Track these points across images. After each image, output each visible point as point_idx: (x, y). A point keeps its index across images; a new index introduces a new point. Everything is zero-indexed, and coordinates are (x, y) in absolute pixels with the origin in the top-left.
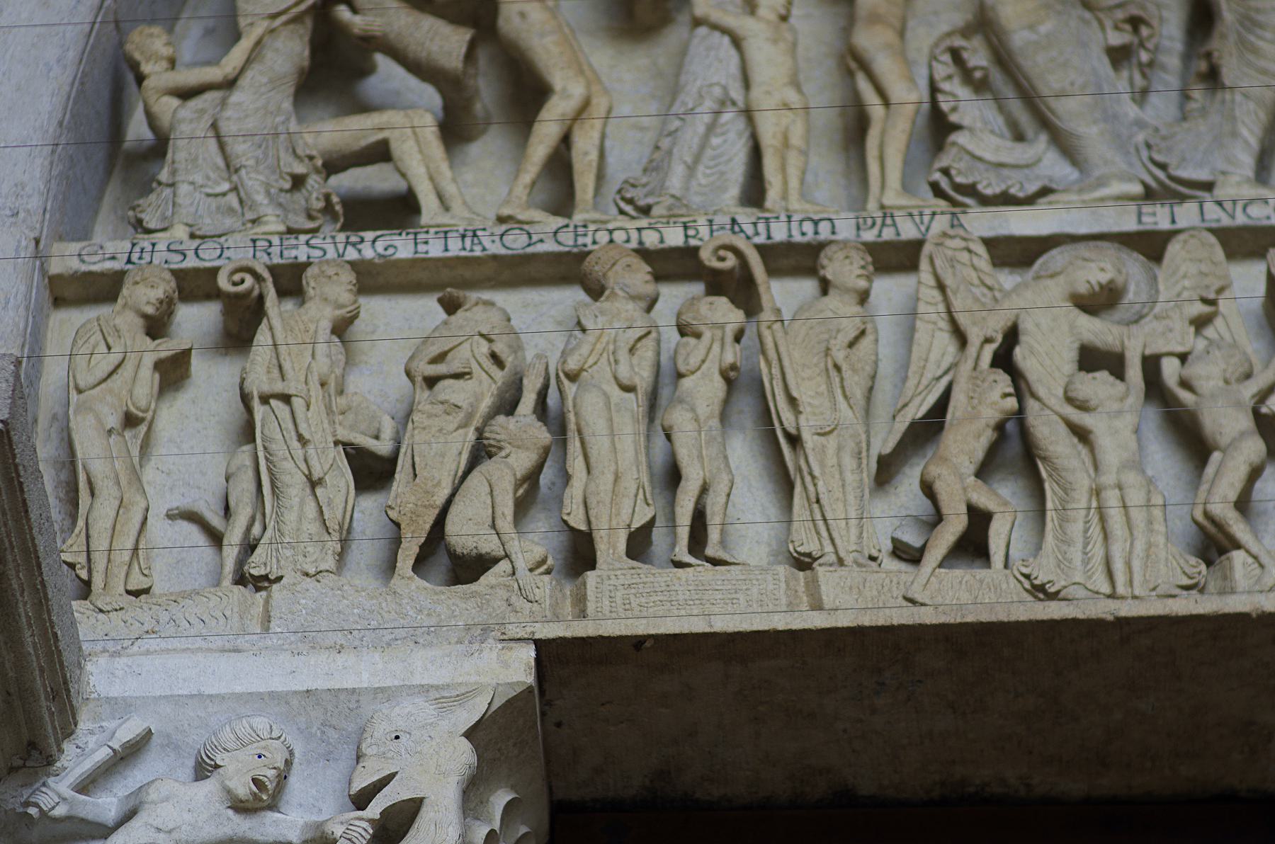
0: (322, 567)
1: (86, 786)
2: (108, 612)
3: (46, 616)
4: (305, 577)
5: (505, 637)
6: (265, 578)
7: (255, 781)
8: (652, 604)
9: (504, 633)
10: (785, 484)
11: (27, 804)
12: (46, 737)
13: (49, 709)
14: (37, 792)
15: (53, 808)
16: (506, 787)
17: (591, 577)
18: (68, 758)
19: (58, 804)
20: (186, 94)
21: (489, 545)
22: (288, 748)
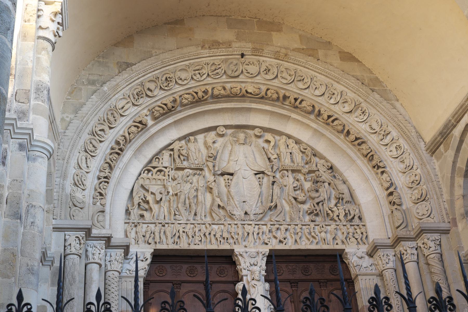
10: (167, 239)
21: (151, 242)
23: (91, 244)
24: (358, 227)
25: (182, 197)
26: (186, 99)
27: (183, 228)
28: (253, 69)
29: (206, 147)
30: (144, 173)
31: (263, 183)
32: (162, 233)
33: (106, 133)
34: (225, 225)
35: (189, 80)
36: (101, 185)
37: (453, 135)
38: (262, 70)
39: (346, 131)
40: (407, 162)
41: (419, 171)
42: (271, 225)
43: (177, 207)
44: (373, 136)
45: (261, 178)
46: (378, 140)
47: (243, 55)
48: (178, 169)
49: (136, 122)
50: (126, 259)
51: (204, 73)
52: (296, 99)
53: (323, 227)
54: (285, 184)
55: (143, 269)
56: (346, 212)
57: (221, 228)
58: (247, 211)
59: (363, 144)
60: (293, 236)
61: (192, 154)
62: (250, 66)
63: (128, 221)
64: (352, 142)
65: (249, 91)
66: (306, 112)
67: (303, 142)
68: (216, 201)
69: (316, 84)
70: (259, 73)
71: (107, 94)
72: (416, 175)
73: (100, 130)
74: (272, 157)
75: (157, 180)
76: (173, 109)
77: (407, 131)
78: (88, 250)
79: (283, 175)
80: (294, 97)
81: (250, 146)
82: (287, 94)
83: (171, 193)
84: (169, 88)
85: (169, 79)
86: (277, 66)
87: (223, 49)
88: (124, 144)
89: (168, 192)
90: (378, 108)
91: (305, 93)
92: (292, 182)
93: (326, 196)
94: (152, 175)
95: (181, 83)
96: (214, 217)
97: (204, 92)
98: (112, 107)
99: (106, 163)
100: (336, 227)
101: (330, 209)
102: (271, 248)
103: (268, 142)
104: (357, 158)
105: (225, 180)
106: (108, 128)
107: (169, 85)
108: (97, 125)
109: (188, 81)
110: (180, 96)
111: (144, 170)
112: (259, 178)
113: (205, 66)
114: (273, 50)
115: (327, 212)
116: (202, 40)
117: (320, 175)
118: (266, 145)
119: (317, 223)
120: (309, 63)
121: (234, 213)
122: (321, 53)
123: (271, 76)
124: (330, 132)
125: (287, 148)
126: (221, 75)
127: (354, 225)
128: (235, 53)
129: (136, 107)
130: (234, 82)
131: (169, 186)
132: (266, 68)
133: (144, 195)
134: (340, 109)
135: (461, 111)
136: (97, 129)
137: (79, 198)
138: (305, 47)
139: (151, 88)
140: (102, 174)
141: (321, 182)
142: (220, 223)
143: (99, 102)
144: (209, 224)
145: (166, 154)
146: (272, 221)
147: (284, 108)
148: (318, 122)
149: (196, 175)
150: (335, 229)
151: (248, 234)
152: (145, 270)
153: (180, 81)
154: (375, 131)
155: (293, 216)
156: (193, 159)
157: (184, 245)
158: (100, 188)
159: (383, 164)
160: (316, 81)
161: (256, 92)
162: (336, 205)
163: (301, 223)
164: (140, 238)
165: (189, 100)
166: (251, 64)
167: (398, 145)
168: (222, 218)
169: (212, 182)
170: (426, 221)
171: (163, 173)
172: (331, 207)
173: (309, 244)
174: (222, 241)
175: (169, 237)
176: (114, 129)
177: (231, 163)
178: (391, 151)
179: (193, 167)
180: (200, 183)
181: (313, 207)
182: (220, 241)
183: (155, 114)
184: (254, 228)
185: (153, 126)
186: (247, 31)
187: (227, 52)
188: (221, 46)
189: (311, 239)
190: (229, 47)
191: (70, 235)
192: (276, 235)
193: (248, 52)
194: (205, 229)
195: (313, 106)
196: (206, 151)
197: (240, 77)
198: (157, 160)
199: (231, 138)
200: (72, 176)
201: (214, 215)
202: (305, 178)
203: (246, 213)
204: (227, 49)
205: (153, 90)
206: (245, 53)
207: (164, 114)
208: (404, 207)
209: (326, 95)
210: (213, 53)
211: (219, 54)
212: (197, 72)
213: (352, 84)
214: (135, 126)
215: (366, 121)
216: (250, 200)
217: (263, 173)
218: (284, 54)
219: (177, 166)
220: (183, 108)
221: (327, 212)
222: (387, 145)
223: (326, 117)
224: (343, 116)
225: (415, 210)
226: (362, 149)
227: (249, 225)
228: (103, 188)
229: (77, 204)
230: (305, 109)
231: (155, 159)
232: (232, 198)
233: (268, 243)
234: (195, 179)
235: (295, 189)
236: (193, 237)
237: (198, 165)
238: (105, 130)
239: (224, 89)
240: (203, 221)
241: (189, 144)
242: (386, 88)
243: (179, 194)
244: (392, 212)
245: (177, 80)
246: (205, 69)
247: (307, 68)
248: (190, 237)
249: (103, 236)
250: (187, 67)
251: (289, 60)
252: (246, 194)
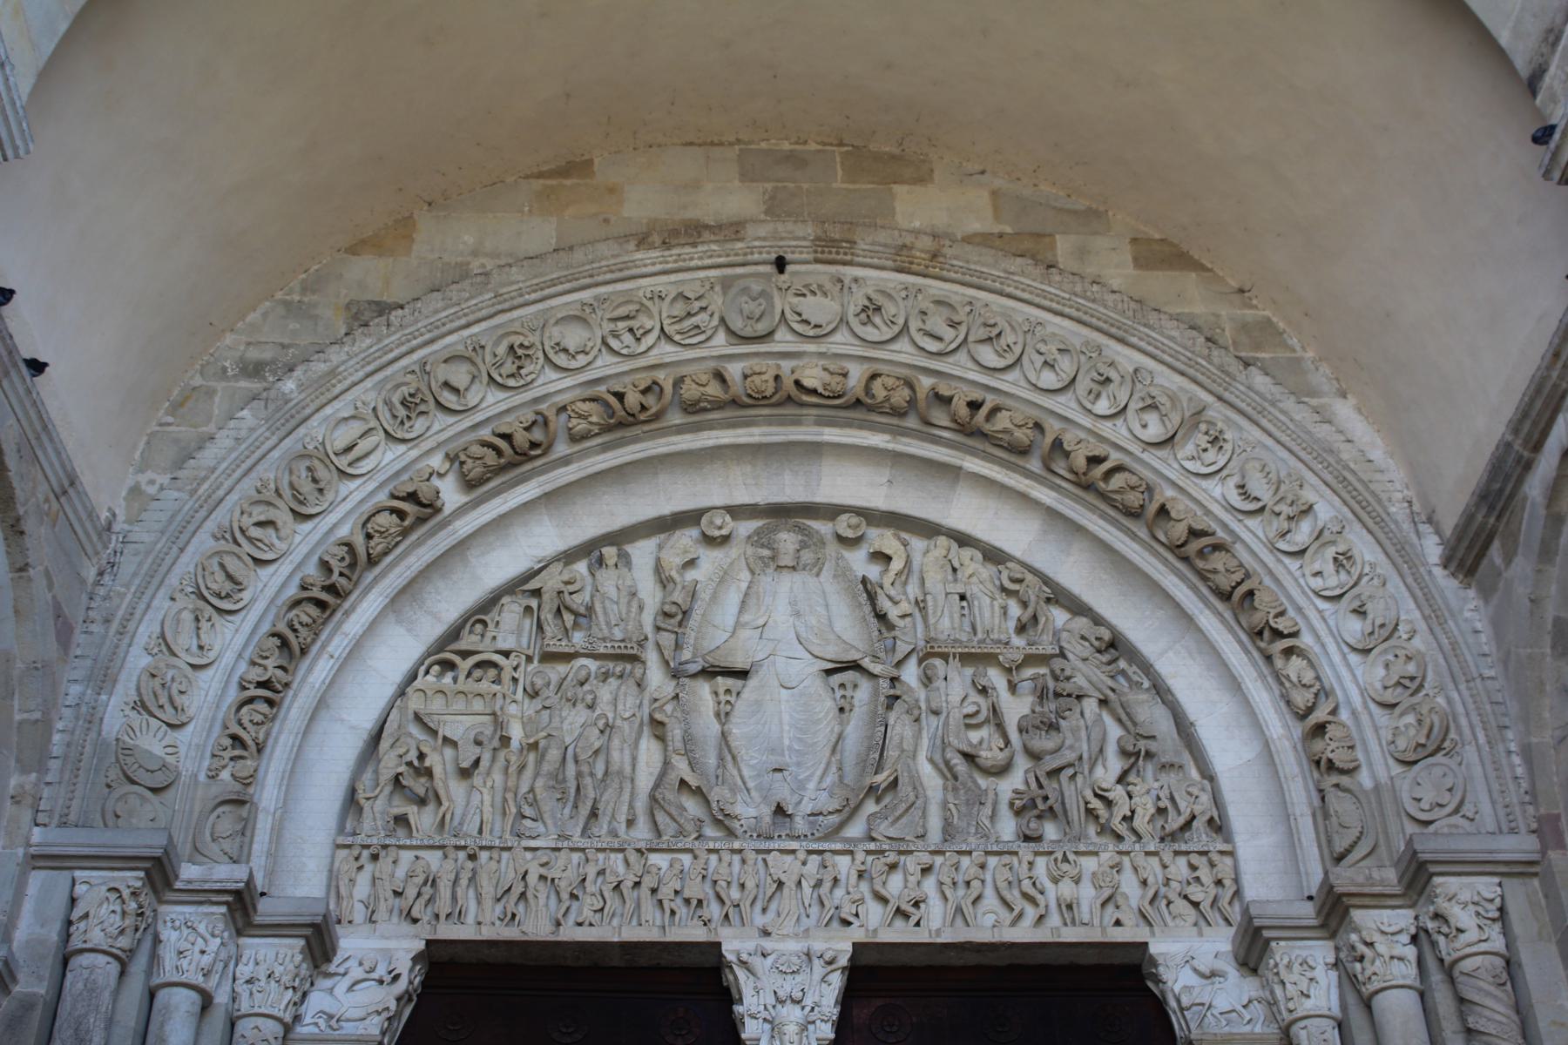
10: (479, 903)
20: (368, 799)
21: (419, 916)
23: (174, 916)
24: (1204, 859)
25: (554, 754)
26: (580, 416)
27: (542, 865)
28: (819, 309)
29: (662, 582)
30: (427, 672)
31: (856, 702)
32: (464, 882)
33: (283, 533)
34: (697, 852)
35: (596, 350)
36: (245, 710)
37: (1525, 499)
38: (852, 310)
39: (1152, 508)
40: (1376, 611)
41: (1417, 643)
42: (868, 852)
43: (532, 790)
44: (1252, 523)
45: (849, 686)
46: (1271, 535)
47: (781, 264)
48: (549, 657)
49: (397, 498)
51: (649, 327)
52: (974, 406)
53: (1065, 859)
54: (934, 706)
55: (379, 1013)
56: (1161, 804)
57: (677, 866)
58: (783, 804)
59: (1217, 553)
60: (948, 893)
61: (604, 608)
62: (810, 298)
63: (348, 841)
64: (1179, 547)
65: (808, 383)
66: (1010, 451)
67: (1011, 558)
68: (673, 767)
69: (1042, 350)
70: (843, 321)
71: (291, 404)
72: (1409, 658)
73: (259, 524)
74: (893, 613)
75: (470, 696)
76: (538, 452)
77: (1370, 499)
78: (162, 937)
79: (929, 672)
80: (969, 399)
81: (818, 575)
82: (945, 391)
83: (515, 744)
84: (522, 382)
85: (520, 352)
86: (903, 294)
87: (714, 247)
88: (346, 571)
89: (505, 741)
90: (1264, 422)
91: (1009, 382)
92: (959, 699)
93: (1085, 747)
94: (455, 680)
95: (564, 366)
96: (661, 827)
97: (645, 392)
98: (310, 447)
99: (273, 635)
100: (1117, 858)
101: (1096, 795)
102: (857, 934)
103: (883, 558)
104: (1201, 605)
105: (716, 693)
106: (289, 517)
107: (523, 372)
108: (245, 506)
109: (590, 358)
110: (563, 409)
111: (427, 662)
112: (842, 686)
113: (649, 304)
114: (889, 241)
115: (1086, 803)
116: (645, 221)
117: (1068, 673)
118: (873, 571)
119: (1044, 847)
120: (1016, 278)
121: (739, 809)
122: (1063, 246)
123: (884, 328)
124: (1104, 516)
125: (950, 577)
126: (709, 333)
127: (1187, 853)
128: (756, 257)
129: (402, 448)
130: (756, 354)
131: (512, 716)
132: (867, 303)
133: (418, 749)
134: (1131, 432)
135: (1538, 404)
136: (247, 521)
137: (150, 753)
138: (1008, 230)
139: (455, 382)
140: (256, 674)
141: (1069, 695)
142: (680, 845)
143: (263, 429)
144: (639, 851)
145: (510, 613)
146: (873, 839)
147: (937, 440)
148: (1059, 481)
149: (611, 680)
150: (1112, 867)
151: (780, 884)
152: (385, 1015)
153: (563, 356)
154: (1260, 504)
155: (956, 821)
156: (608, 623)
157: (536, 926)
158: (240, 723)
159: (1289, 623)
160: (1044, 341)
161: (833, 384)
162: (1121, 780)
163: (982, 847)
164: (382, 900)
165: (594, 419)
166: (814, 293)
167: (1340, 551)
168: (689, 827)
169: (664, 700)
170: (1446, 830)
171: (492, 672)
172: (1104, 786)
173: (1008, 922)
174: (682, 911)
175: (488, 902)
176: (316, 520)
177: (744, 634)
178: (1318, 574)
179: (602, 650)
180: (620, 707)
181: (1034, 785)
182: (673, 913)
183: (466, 467)
184: (804, 863)
185: (461, 511)
186: (805, 186)
187: (728, 256)
188: (706, 235)
189: (1019, 903)
190: (734, 237)
191: (93, 881)
192: (883, 892)
193: (801, 253)
194: (621, 869)
195: (1038, 426)
196: (659, 595)
197: (778, 336)
198: (479, 627)
199: (750, 550)
200: (135, 679)
201: (661, 818)
202: (1009, 682)
203: (780, 811)
204: (729, 246)
205: (462, 389)
206: (788, 257)
207: (502, 469)
208: (1365, 779)
209: (1083, 384)
210: (676, 261)
211: (700, 263)
212: (621, 325)
213: (1172, 344)
214: (393, 511)
215: (1224, 473)
216: (798, 764)
217: (855, 666)
218: (927, 252)
219: (549, 649)
220: (577, 448)
221: (1086, 803)
222: (1302, 552)
223: (1080, 462)
224: (1145, 456)
225: (1406, 787)
226: (1215, 571)
227: (782, 851)
228: (251, 721)
229: (141, 776)
230: (1005, 437)
231: (473, 625)
232: (734, 758)
233: (851, 919)
234: (605, 693)
235: (973, 721)
236: (573, 896)
237: (622, 645)
238: (280, 524)
239: (720, 377)
240: (616, 840)
241: (598, 574)
242: (1300, 353)
243: (542, 743)
244: (1323, 799)
245: (551, 355)
246: (651, 316)
247: (1009, 296)
248: (565, 896)
249: (217, 886)
250: (588, 310)
251: (945, 273)
252: (787, 742)
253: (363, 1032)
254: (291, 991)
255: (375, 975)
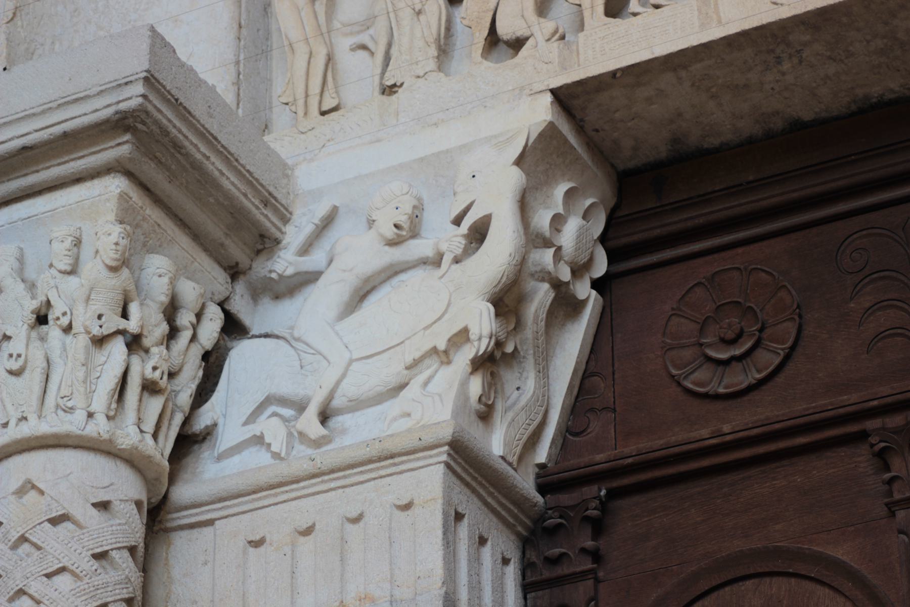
0: (427, 70)
1: (305, 249)
2: (306, 132)
3: (236, 164)
4: (418, 79)
5: (532, 92)
6: (394, 85)
7: (396, 226)
8: (617, 47)
9: (531, 90)
11: (271, 271)
12: (267, 230)
13: (263, 214)
14: (275, 263)
15: (285, 271)
16: (564, 182)
17: (581, 35)
18: (290, 236)
19: (287, 267)
21: (521, 32)
22: (415, 197)
50: (277, 297)
55: (444, 356)
253: (403, 425)
254: (118, 349)
255: (420, 248)
